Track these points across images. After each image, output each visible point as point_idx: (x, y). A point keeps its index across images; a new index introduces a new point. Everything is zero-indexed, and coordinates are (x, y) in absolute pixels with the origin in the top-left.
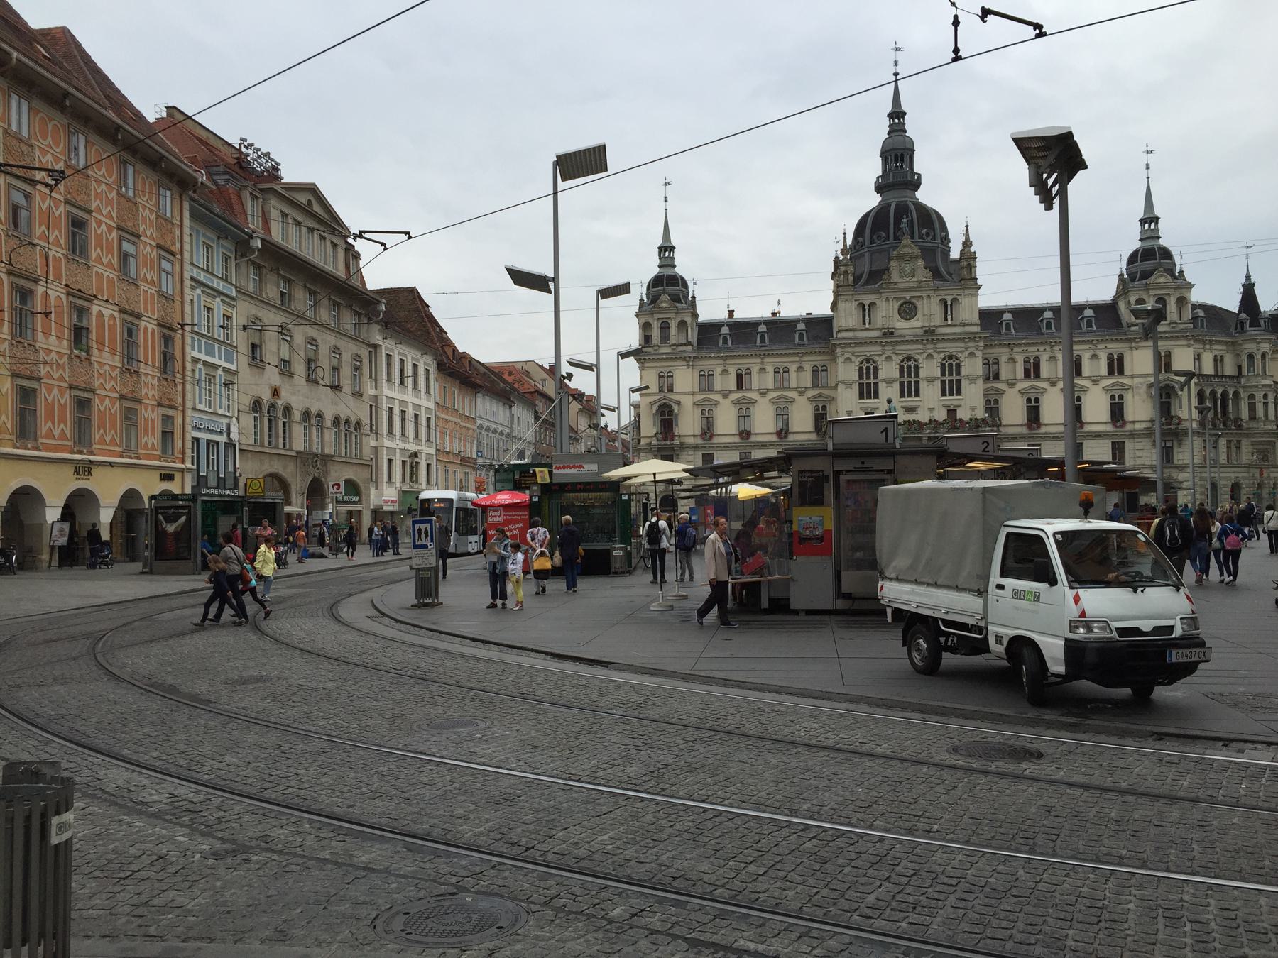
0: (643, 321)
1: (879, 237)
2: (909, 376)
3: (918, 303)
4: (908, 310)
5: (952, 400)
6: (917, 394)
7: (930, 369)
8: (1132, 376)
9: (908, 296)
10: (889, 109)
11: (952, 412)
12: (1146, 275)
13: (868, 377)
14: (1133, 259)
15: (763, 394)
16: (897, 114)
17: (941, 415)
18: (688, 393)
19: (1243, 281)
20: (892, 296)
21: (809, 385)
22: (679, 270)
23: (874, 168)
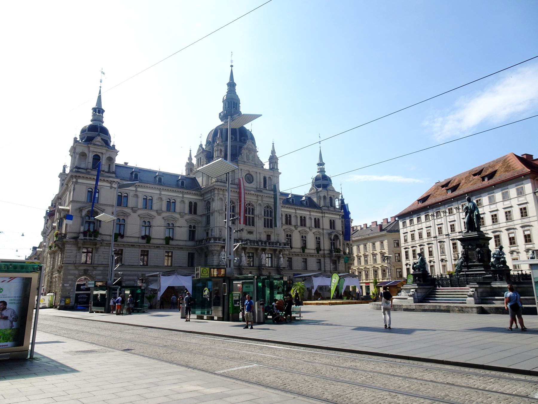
3: (254, 176)
5: (269, 230)
6: (253, 225)
11: (269, 237)
14: (317, 179)
15: (159, 214)
16: (232, 85)
17: (264, 238)
18: (110, 205)
23: (220, 108)
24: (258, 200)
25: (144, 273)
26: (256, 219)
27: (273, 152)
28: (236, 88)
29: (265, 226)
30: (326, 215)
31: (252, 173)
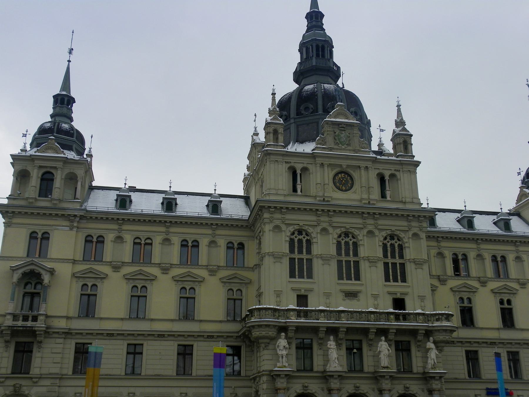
0: (19, 168)
1: (307, 108)
2: (347, 254)
3: (355, 175)
4: (344, 180)
6: (358, 278)
7: (370, 248)
9: (344, 163)
10: (307, 9)
13: (300, 252)
15: (165, 270)
20: (326, 161)
22: (77, 124)
25: (132, 390)
26: (364, 266)
27: (400, 123)
28: (324, 21)
29: (387, 279)
31: (351, 172)
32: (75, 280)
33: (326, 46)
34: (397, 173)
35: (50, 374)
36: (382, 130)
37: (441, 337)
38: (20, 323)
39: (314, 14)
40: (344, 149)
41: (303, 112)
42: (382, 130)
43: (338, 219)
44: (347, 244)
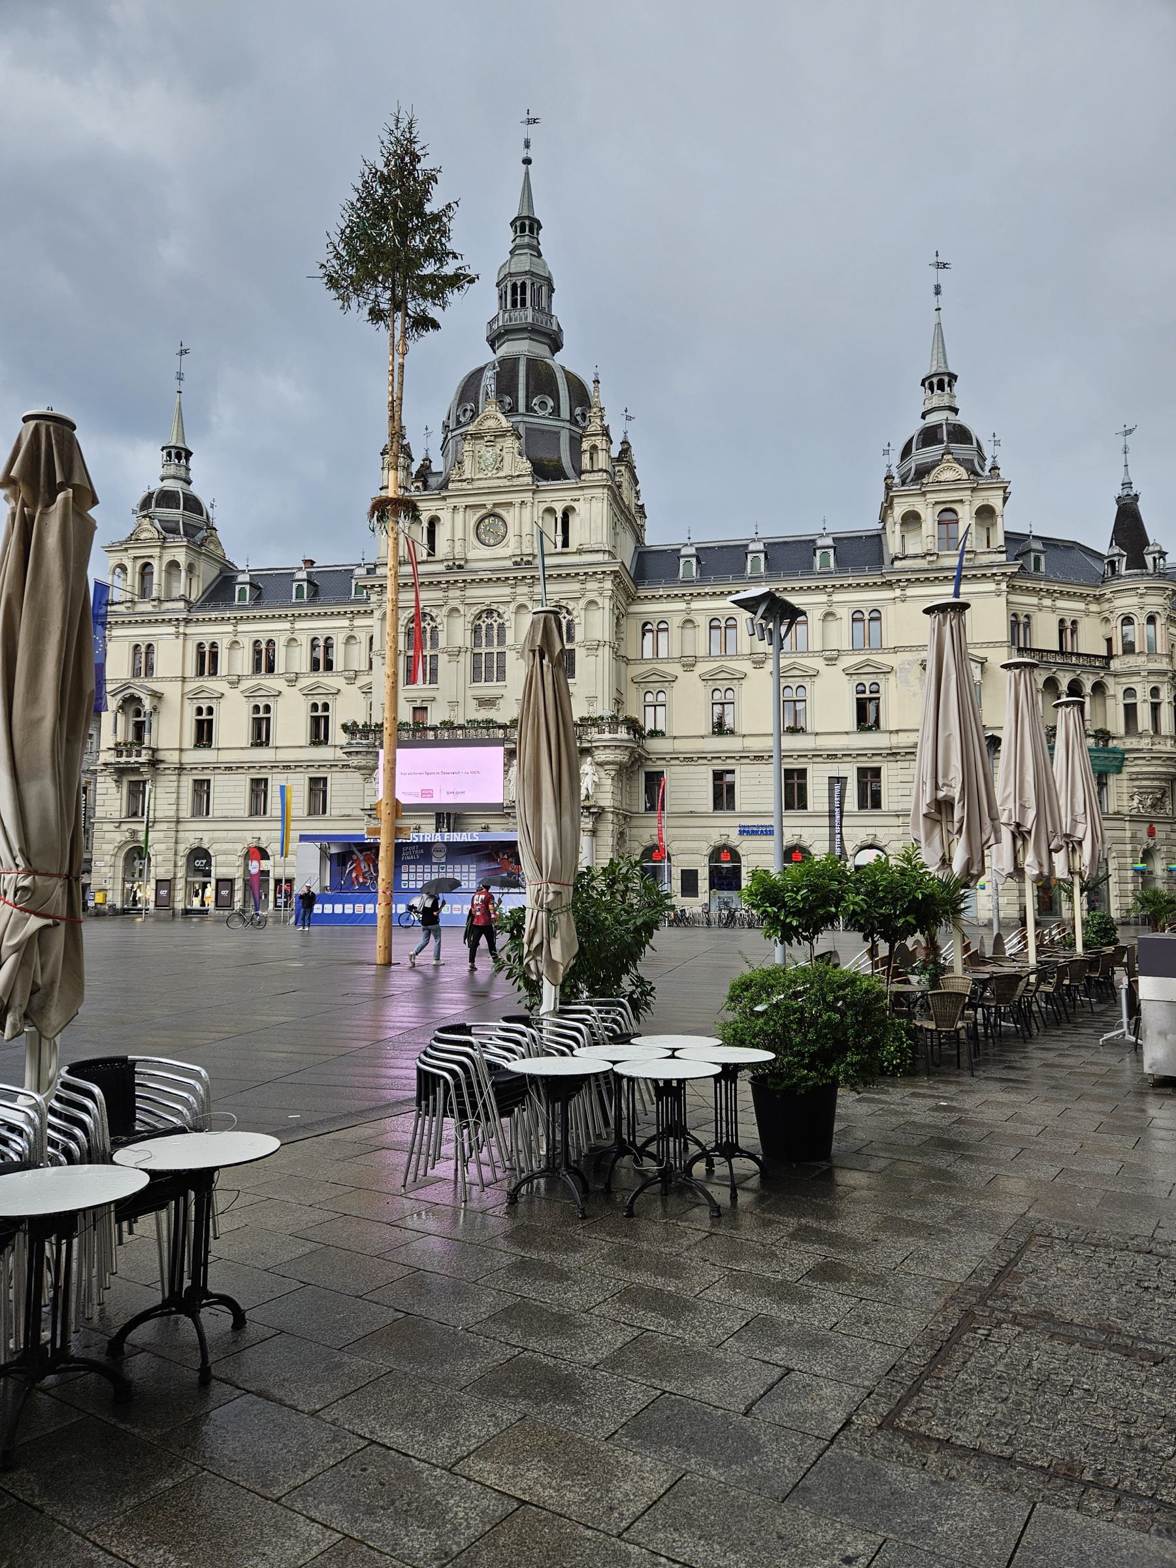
2: (489, 643)
8: (895, 650)
12: (923, 472)
19: (1119, 491)
20: (462, 502)
21: (364, 666)
24: (514, 596)
25: (257, 834)
30: (910, 592)
32: (187, 702)
33: (529, 283)
34: (574, 504)
35: (166, 817)
36: (629, 418)
37: (601, 756)
38: (123, 759)
39: (518, 224)
40: (490, 478)
41: (462, 419)
42: (629, 418)
43: (473, 592)
44: (486, 627)
